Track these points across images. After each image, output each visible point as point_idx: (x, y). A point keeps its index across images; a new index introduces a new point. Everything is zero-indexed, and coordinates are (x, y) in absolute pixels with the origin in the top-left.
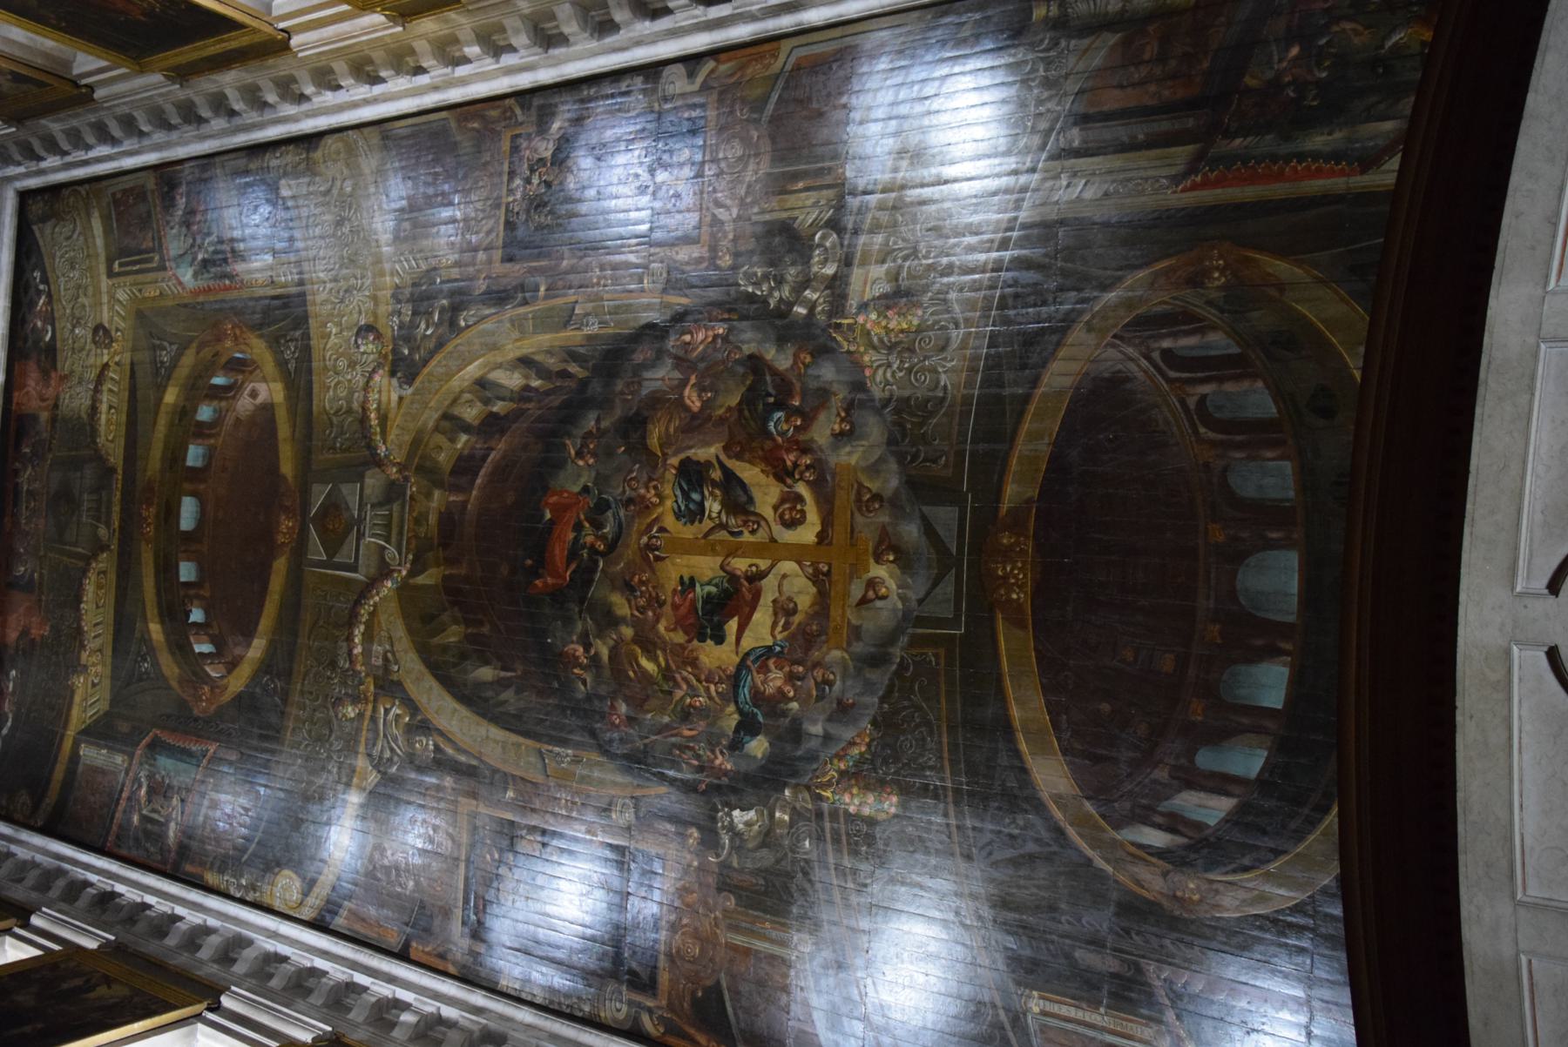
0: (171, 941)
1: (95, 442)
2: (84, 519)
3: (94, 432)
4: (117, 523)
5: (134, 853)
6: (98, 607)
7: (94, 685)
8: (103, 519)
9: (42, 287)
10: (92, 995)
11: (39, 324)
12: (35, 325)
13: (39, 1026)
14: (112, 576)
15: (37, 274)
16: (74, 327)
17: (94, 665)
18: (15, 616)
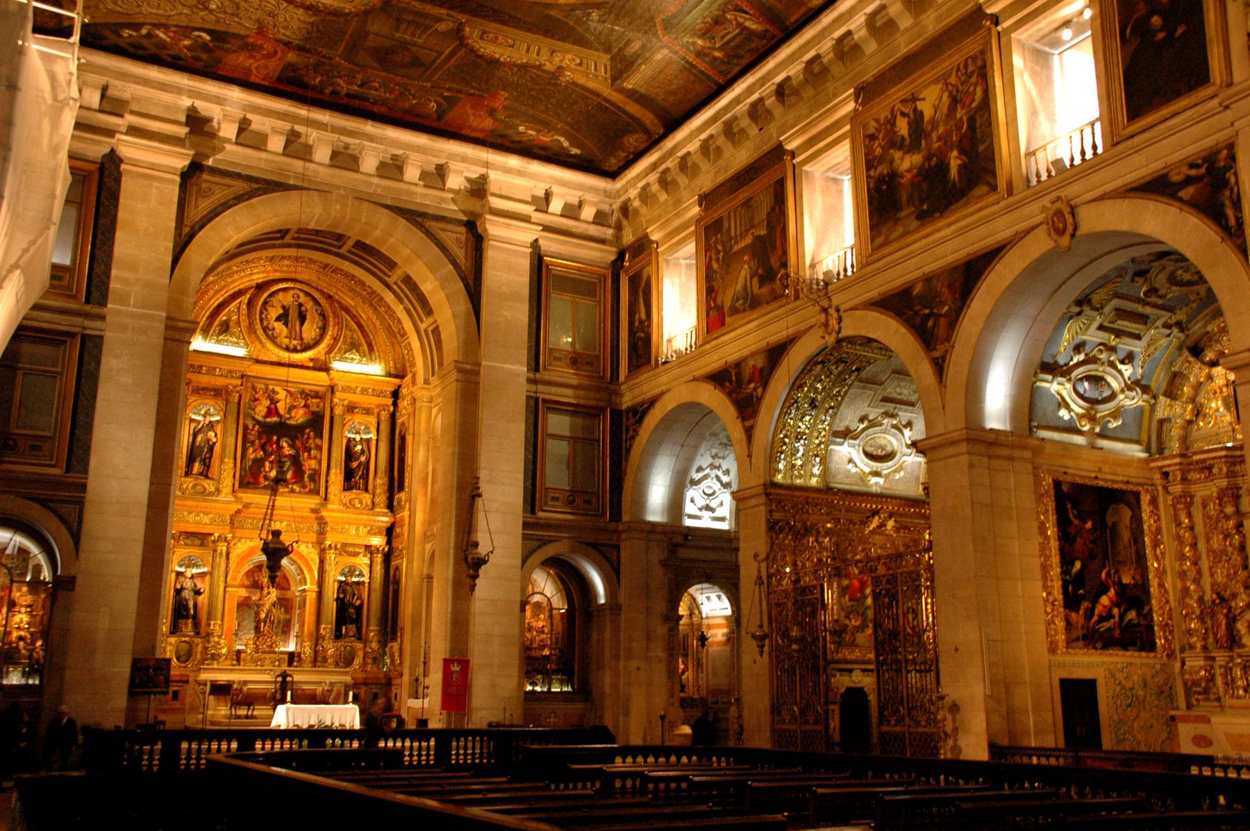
0: (871, 47)
1: (347, 14)
2: (420, 41)
3: (336, 13)
4: (444, 12)
5: (744, 62)
6: (512, 46)
7: (580, 64)
8: (427, 22)
9: (144, 31)
10: (928, 113)
11: (187, 42)
12: (185, 47)
13: (955, 153)
14: (493, 26)
15: (126, 33)
16: (206, 8)
17: (561, 61)
18: (472, 118)
